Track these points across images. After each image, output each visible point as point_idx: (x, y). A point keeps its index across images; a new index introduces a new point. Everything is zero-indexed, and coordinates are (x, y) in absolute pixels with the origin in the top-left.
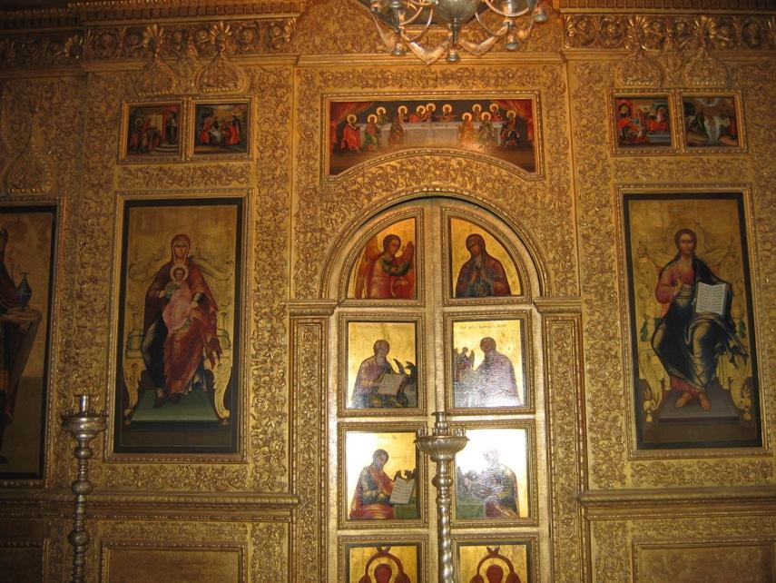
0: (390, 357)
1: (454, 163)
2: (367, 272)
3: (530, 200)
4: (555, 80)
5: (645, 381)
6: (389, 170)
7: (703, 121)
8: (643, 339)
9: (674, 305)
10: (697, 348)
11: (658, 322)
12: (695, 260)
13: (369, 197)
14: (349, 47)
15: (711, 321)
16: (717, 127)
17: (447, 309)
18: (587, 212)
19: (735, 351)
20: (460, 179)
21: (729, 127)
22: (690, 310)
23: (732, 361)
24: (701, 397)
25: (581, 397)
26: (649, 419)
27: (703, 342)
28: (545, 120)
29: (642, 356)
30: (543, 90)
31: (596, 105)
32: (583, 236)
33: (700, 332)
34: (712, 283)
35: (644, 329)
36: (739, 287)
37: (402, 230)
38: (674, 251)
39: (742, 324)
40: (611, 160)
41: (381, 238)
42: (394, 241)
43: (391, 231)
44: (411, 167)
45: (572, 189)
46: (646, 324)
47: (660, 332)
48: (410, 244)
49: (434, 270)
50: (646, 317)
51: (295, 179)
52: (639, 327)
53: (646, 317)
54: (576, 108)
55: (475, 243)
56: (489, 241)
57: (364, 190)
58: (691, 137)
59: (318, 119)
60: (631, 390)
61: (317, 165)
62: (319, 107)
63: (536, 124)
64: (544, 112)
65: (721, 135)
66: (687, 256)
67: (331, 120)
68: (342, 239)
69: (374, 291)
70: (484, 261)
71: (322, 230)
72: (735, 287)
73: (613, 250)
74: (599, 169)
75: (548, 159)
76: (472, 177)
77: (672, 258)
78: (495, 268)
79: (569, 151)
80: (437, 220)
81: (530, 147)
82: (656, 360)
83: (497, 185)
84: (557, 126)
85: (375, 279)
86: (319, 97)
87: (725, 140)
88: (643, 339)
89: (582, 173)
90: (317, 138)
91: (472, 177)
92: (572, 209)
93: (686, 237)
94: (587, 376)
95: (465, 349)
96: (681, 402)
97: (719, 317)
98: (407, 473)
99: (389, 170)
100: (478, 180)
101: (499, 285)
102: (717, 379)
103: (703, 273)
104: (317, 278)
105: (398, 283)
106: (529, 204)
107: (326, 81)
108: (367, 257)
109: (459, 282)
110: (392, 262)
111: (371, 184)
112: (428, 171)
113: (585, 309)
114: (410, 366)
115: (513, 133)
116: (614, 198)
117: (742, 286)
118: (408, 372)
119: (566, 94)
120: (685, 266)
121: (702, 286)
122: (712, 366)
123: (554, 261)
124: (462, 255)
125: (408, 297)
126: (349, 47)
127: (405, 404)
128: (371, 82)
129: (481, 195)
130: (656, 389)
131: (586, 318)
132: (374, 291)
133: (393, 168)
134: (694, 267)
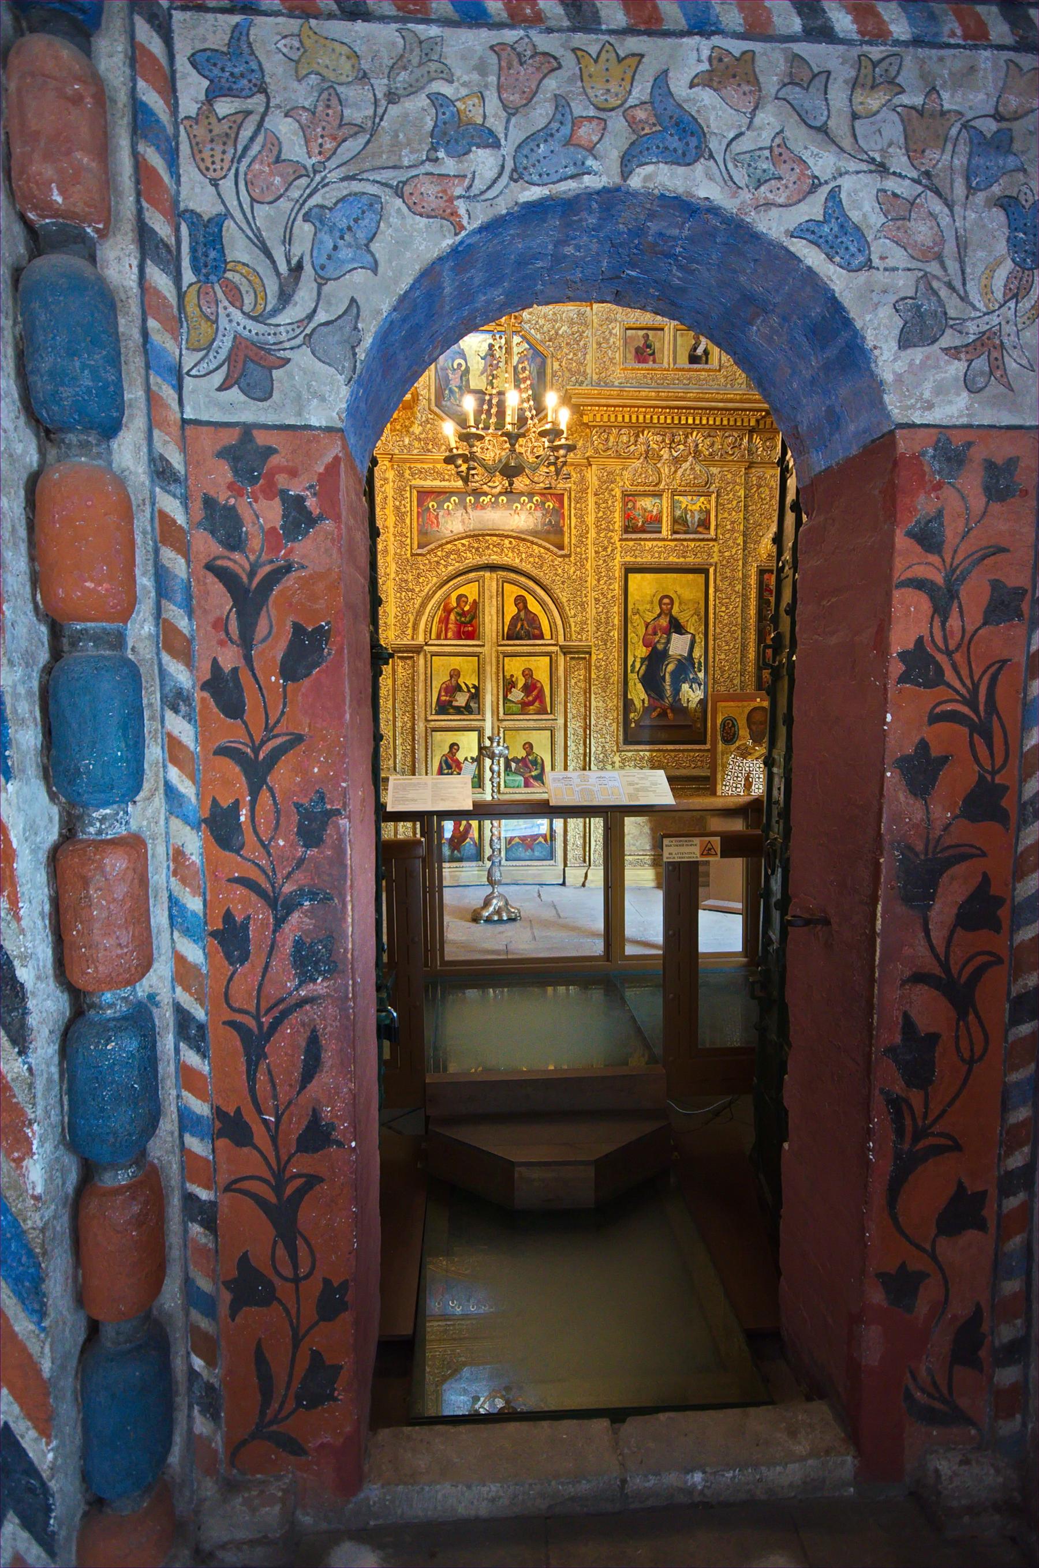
0: (461, 681)
1: (507, 542)
2: (445, 621)
3: (560, 571)
4: (583, 479)
5: (632, 700)
6: (460, 546)
7: (686, 514)
8: (632, 672)
9: (654, 648)
10: (667, 676)
11: (643, 660)
12: (671, 617)
13: (446, 566)
14: (430, 447)
15: (679, 660)
16: (696, 519)
17: (500, 648)
18: (599, 581)
19: (695, 680)
20: (510, 554)
21: (705, 520)
22: (666, 651)
23: (691, 687)
24: (669, 711)
25: (588, 708)
26: (633, 725)
27: (672, 673)
28: (573, 511)
29: (631, 684)
30: (574, 487)
31: (610, 502)
32: (596, 599)
33: (671, 667)
34: (681, 634)
35: (633, 665)
36: (700, 638)
37: (471, 591)
38: (658, 611)
39: (700, 663)
40: (618, 544)
41: (454, 596)
42: (464, 599)
43: (460, 591)
44: (476, 545)
45: (589, 564)
46: (634, 662)
47: (644, 667)
48: (475, 600)
49: (492, 620)
50: (635, 657)
51: (393, 552)
52: (630, 663)
53: (635, 657)
54: (596, 503)
55: (520, 601)
56: (530, 599)
57: (442, 562)
58: (677, 527)
59: (408, 505)
60: (621, 704)
61: (408, 541)
62: (408, 495)
63: (566, 513)
64: (573, 505)
65: (698, 526)
66: (666, 615)
67: (418, 506)
68: (428, 598)
69: (450, 634)
70: (526, 614)
71: (413, 590)
72: (698, 640)
73: (616, 609)
74: (609, 550)
75: (573, 542)
76: (520, 553)
77: (655, 615)
78: (533, 620)
79: (589, 535)
80: (494, 584)
81: (562, 533)
82: (640, 686)
83: (537, 560)
84: (582, 516)
85: (450, 626)
86: (408, 488)
87: (700, 529)
88: (632, 672)
89: (596, 552)
90: (408, 521)
91: (520, 553)
92: (589, 579)
93: (666, 601)
94: (593, 696)
95: (512, 676)
96: (655, 714)
97: (685, 658)
98: (472, 758)
99: (460, 546)
100: (524, 555)
101: (537, 632)
102: (680, 699)
103: (677, 627)
104: (410, 625)
105: (466, 629)
106: (557, 575)
107: (413, 475)
108: (444, 610)
109: (509, 629)
110: (463, 614)
111: (448, 557)
112: (488, 548)
113: (593, 650)
114: (474, 687)
115: (550, 521)
116: (618, 573)
117: (702, 636)
118: (473, 691)
119: (589, 491)
120: (664, 622)
121: (675, 636)
122: (677, 691)
123: (575, 616)
124: (511, 610)
125: (473, 639)
126: (430, 447)
127: (471, 713)
128: (447, 477)
129: (526, 567)
130: (638, 704)
131: (594, 657)
132: (450, 634)
133: (463, 545)
134: (670, 622)
